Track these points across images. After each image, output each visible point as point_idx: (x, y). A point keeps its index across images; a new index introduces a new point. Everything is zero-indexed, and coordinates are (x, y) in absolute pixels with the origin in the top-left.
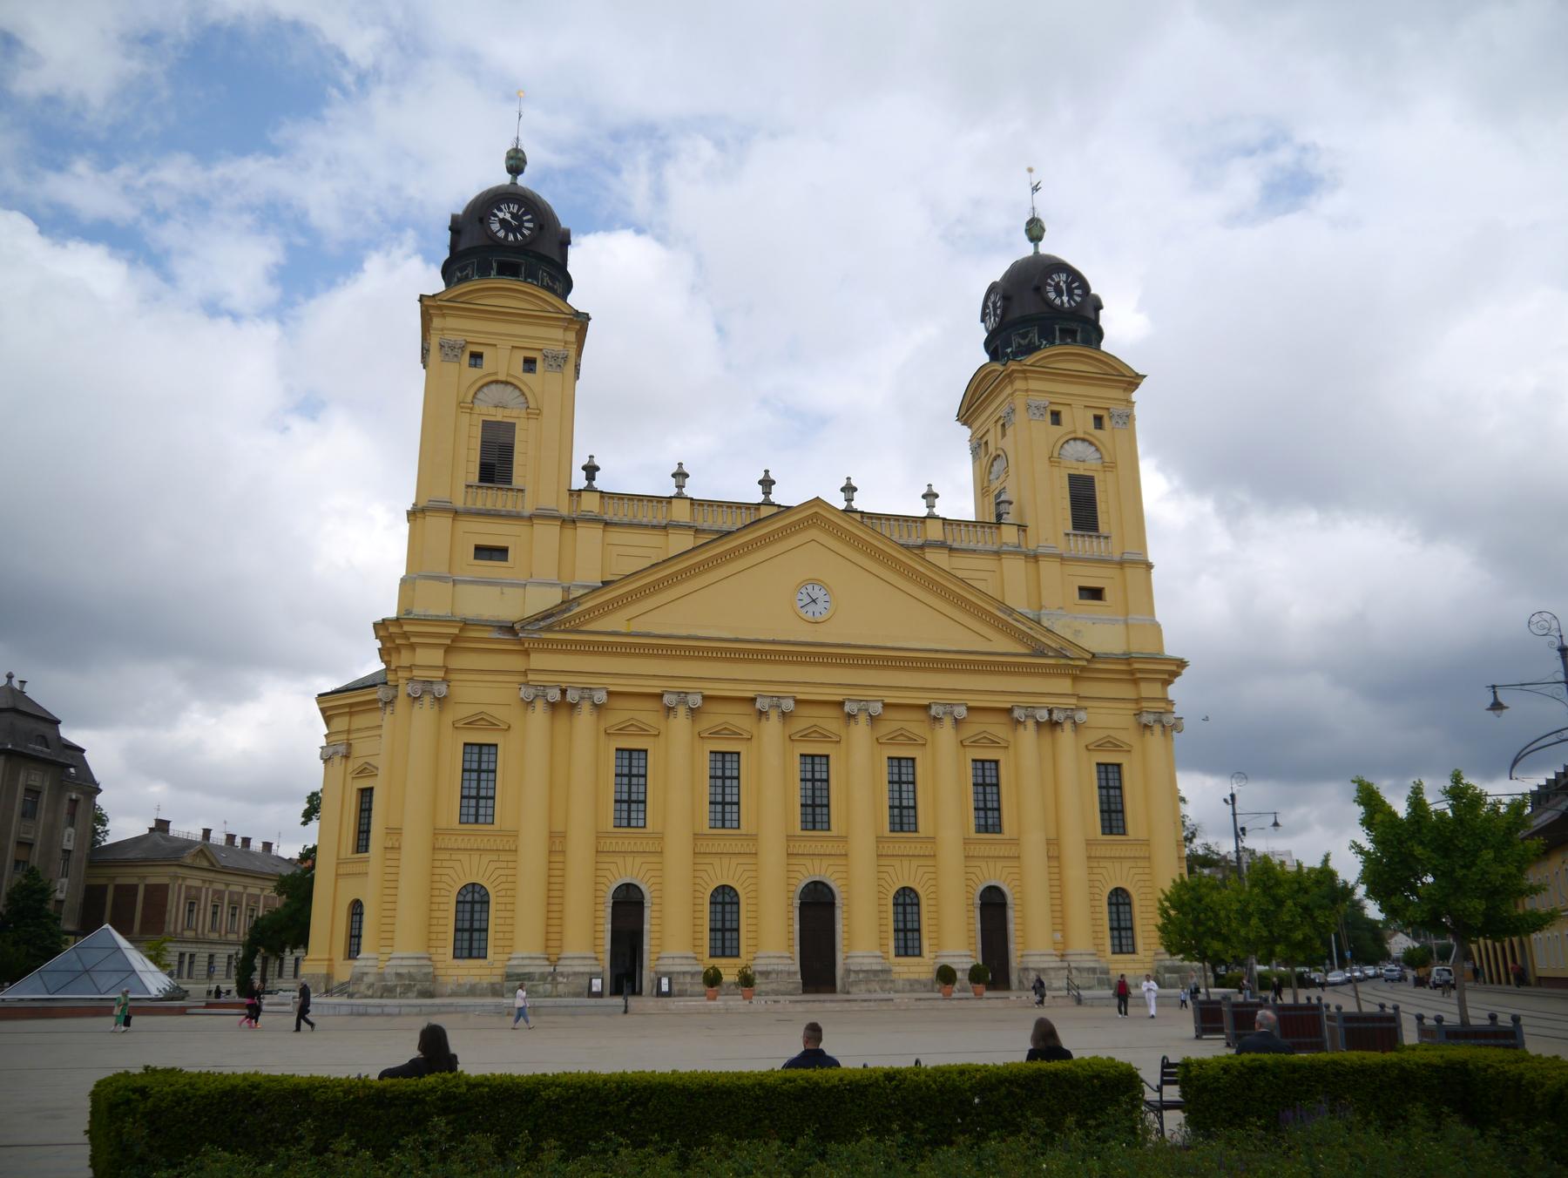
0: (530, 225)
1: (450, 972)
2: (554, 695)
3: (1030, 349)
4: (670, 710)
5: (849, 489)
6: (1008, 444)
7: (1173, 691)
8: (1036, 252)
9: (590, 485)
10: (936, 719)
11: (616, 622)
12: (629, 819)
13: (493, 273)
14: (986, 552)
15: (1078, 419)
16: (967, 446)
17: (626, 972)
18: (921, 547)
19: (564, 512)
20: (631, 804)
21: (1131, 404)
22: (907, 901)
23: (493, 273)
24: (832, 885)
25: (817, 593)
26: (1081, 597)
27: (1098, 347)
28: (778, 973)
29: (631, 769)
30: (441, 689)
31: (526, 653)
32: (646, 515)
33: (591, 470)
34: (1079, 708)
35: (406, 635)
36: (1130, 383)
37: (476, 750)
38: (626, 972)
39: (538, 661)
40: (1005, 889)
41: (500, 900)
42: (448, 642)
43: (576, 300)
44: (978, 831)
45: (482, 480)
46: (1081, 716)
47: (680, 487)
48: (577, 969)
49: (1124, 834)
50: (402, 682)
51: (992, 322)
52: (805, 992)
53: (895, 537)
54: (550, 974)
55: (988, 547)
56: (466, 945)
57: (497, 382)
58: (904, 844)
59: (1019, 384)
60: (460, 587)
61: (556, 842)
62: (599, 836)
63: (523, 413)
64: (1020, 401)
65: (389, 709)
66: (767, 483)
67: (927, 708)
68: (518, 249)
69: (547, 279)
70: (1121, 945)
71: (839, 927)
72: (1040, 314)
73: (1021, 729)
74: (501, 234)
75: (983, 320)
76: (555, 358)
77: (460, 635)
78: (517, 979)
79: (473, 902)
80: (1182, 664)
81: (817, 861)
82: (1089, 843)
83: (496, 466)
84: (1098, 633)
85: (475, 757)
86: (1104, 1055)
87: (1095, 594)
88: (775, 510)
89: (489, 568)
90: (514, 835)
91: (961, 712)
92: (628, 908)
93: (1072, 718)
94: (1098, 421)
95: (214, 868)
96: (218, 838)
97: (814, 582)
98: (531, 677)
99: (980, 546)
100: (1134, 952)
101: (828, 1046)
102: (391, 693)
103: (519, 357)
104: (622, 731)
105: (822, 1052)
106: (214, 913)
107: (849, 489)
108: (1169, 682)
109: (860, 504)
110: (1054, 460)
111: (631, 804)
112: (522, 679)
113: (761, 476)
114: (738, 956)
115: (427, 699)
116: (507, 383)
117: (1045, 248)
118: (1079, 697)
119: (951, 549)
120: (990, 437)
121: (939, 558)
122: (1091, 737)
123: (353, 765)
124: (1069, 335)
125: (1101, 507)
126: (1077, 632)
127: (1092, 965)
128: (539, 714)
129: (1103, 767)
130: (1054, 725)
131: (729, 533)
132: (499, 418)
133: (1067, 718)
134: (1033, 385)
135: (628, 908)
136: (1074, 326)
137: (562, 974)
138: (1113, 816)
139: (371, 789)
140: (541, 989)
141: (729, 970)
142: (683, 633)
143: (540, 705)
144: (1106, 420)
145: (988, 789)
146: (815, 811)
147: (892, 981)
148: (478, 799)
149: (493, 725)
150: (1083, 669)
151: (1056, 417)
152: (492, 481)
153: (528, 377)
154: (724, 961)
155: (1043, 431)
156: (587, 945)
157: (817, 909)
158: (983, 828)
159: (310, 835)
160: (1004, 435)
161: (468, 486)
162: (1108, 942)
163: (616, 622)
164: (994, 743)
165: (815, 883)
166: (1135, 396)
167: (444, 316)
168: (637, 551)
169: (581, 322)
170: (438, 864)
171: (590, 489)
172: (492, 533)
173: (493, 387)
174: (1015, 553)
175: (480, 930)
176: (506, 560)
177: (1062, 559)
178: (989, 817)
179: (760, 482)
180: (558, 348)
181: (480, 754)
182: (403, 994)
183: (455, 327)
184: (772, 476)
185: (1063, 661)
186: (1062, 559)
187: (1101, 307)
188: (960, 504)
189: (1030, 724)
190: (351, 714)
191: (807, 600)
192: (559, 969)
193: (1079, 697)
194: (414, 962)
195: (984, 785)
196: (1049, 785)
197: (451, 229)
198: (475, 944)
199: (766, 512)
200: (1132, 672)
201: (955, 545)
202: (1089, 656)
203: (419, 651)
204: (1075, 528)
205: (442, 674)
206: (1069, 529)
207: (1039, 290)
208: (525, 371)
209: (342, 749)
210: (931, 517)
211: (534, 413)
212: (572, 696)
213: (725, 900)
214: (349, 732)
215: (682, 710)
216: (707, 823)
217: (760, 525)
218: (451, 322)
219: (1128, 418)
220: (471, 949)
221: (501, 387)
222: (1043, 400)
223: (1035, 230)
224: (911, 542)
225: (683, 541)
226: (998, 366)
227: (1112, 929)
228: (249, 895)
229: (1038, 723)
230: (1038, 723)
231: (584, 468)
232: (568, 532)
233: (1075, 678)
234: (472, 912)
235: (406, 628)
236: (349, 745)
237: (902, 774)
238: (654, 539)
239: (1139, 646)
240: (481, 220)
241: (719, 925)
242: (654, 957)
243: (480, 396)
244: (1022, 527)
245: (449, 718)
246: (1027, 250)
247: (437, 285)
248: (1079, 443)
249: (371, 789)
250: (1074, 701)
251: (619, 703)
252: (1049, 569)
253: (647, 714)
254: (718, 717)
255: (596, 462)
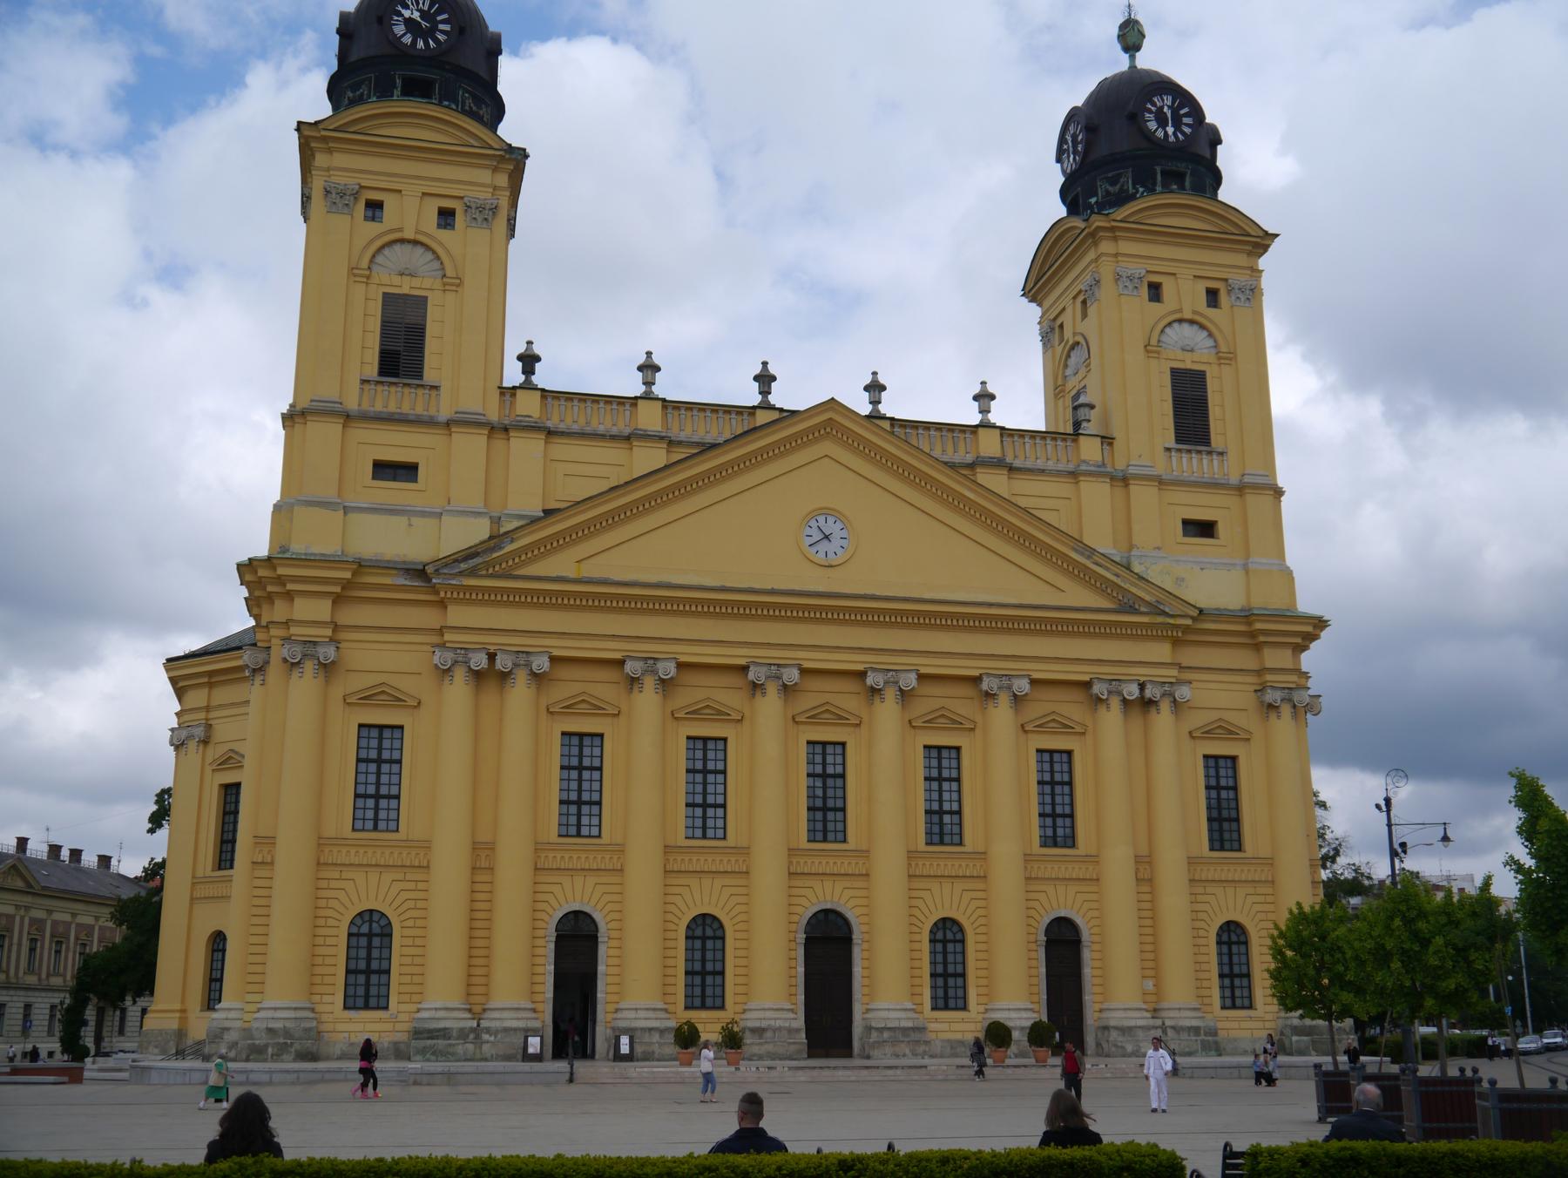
0: (446, 27)
1: (340, 1027)
2: (479, 661)
3: (1122, 199)
4: (633, 682)
5: (875, 388)
6: (1089, 327)
7: (1307, 660)
8: (1133, 67)
9: (528, 381)
10: (989, 695)
11: (561, 564)
12: (579, 825)
13: (397, 92)
14: (1059, 473)
15: (1185, 294)
16: (1035, 331)
17: (573, 1026)
18: (971, 466)
19: (493, 416)
20: (580, 806)
21: (1257, 273)
22: (947, 935)
23: (397, 92)
24: (850, 915)
25: (832, 527)
26: (1185, 534)
27: (1214, 196)
28: (775, 1030)
29: (582, 759)
30: (329, 652)
31: (442, 604)
32: (603, 421)
33: (529, 361)
34: (1180, 682)
35: (281, 580)
36: (1256, 245)
37: (374, 733)
38: (573, 1026)
39: (458, 615)
40: (1079, 920)
41: (407, 932)
42: (338, 589)
43: (509, 131)
44: (1044, 845)
45: (382, 372)
46: (1183, 692)
47: (649, 383)
48: (508, 1024)
49: (961, 844)
50: (274, 641)
51: (1071, 161)
52: (810, 1056)
53: (937, 453)
54: (472, 1030)
55: (1061, 467)
56: (361, 991)
57: (402, 241)
58: (945, 861)
59: (1106, 247)
60: (352, 516)
61: (482, 857)
62: (539, 848)
63: (438, 284)
64: (1106, 270)
65: (258, 679)
66: (765, 380)
67: (976, 680)
68: (428, 59)
69: (469, 102)
70: (1233, 997)
71: (858, 970)
72: (1136, 151)
73: (1102, 710)
74: (408, 39)
75: (1059, 160)
76: (481, 209)
77: (354, 580)
78: (427, 1038)
79: (370, 935)
80: (1321, 623)
81: (828, 884)
82: (1192, 861)
83: (401, 354)
84: (1208, 582)
85: (374, 743)
86: (1142, 1140)
87: (1205, 529)
88: (776, 415)
89: (393, 492)
90: (426, 846)
91: (1022, 686)
92: (577, 943)
93: (1172, 695)
94: (1213, 297)
95: (30, 890)
96: (37, 849)
97: (827, 512)
98: (447, 637)
99: (1051, 465)
100: (1250, 1007)
101: (771, 1125)
102: (261, 657)
103: (432, 207)
104: (569, 709)
105: (763, 1131)
106: (32, 950)
107: (875, 388)
108: (1305, 648)
109: (888, 408)
110: (1151, 349)
111: (580, 806)
112: (435, 639)
113: (758, 370)
114: (722, 1007)
115: (309, 666)
116: (415, 242)
117: (1145, 60)
118: (1181, 667)
119: (1011, 469)
120: (1066, 319)
121: (995, 481)
122: (1197, 720)
123: (214, 752)
124: (1174, 179)
125: (1214, 412)
126: (1179, 581)
127: (1195, 1023)
128: (459, 689)
129: (699, 743)
130: (1147, 704)
131: (714, 446)
132: (405, 290)
133: (1163, 695)
134: (1126, 247)
135: (577, 943)
136: (1181, 166)
137: (488, 1030)
138: (1224, 826)
139: (238, 785)
140: (460, 1049)
141: (710, 1026)
142: (653, 579)
143: (460, 674)
144: (1223, 298)
145: (1058, 789)
146: (826, 813)
147: (927, 1043)
148: (377, 799)
149: (397, 701)
150: (1186, 629)
151: (1155, 292)
152: (396, 375)
153: (444, 235)
154: (704, 1014)
155: (1137, 308)
156: (521, 992)
157: (828, 946)
158: (1050, 841)
159: (158, 846)
160: (1085, 315)
161: (364, 382)
162: (927, 993)
163: (561, 564)
164: (1066, 728)
165: (826, 912)
166: (1263, 262)
167: (330, 151)
168: (590, 469)
169: (515, 159)
170: (324, 884)
171: (528, 386)
172: (397, 445)
173: (397, 247)
174: (1100, 472)
175: (379, 972)
176: (415, 480)
177: (1161, 482)
178: (1058, 824)
179: (756, 378)
180: (484, 195)
181: (381, 739)
182: (276, 1057)
183: (347, 166)
184: (772, 370)
185: (1160, 619)
186: (1161, 482)
187: (1220, 142)
188: (1024, 406)
189: (1115, 703)
190: (211, 685)
191: (817, 536)
192: (484, 1024)
193: (1181, 667)
194: (291, 1014)
195: (1053, 783)
196: (1139, 783)
197: (338, 31)
198: (373, 990)
199: (763, 417)
200: (1253, 634)
201: (1017, 463)
202: (1195, 613)
203: (298, 602)
204: (1178, 441)
205: (329, 632)
206: (1171, 443)
207: (1135, 118)
208: (439, 226)
209: (199, 732)
210: (985, 425)
211: (452, 283)
212: (503, 662)
213: (706, 934)
214: (208, 709)
215: (649, 682)
216: (682, 832)
217: (754, 436)
218: (339, 160)
219: (1252, 293)
220: (367, 996)
221: (408, 247)
222: (1137, 268)
223: (1131, 36)
224: (957, 459)
225: (650, 458)
226: (1078, 223)
227: (1221, 976)
228: (78, 925)
229: (1125, 701)
230: (1124, 701)
231: (520, 358)
232: (499, 443)
233: (1176, 643)
234: (369, 947)
235: (281, 571)
236: (209, 727)
237: (943, 768)
239: (1265, 599)
240: (380, 20)
241: (698, 967)
242: (611, 1007)
243: (379, 259)
244: (1107, 440)
245: (337, 692)
247: (320, 108)
248: (1186, 326)
249: (238, 785)
250: (1174, 672)
251: (565, 672)
252: (1142, 495)
253: (603, 688)
254: (698, 691)
255: (537, 350)
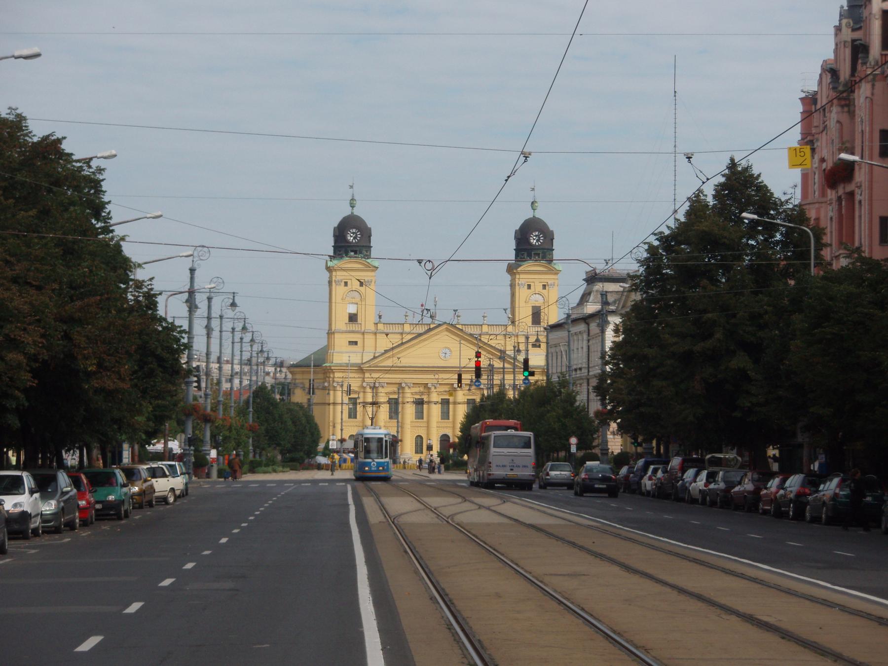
18: (480, 335)
77: (345, 368)
94: (544, 287)
134: (522, 276)
136: (539, 252)
172: (354, 337)
180: (369, 279)
199: (432, 326)
238: (399, 336)
246: (529, 214)
